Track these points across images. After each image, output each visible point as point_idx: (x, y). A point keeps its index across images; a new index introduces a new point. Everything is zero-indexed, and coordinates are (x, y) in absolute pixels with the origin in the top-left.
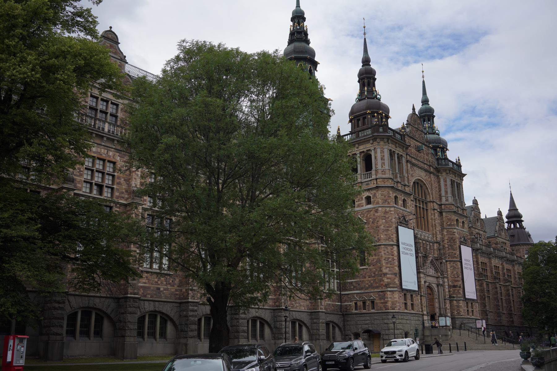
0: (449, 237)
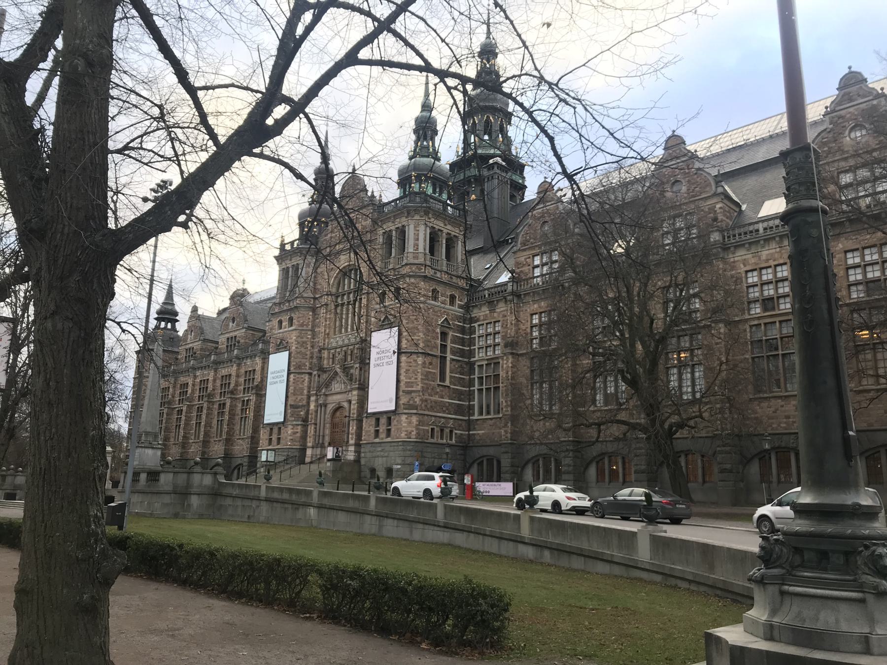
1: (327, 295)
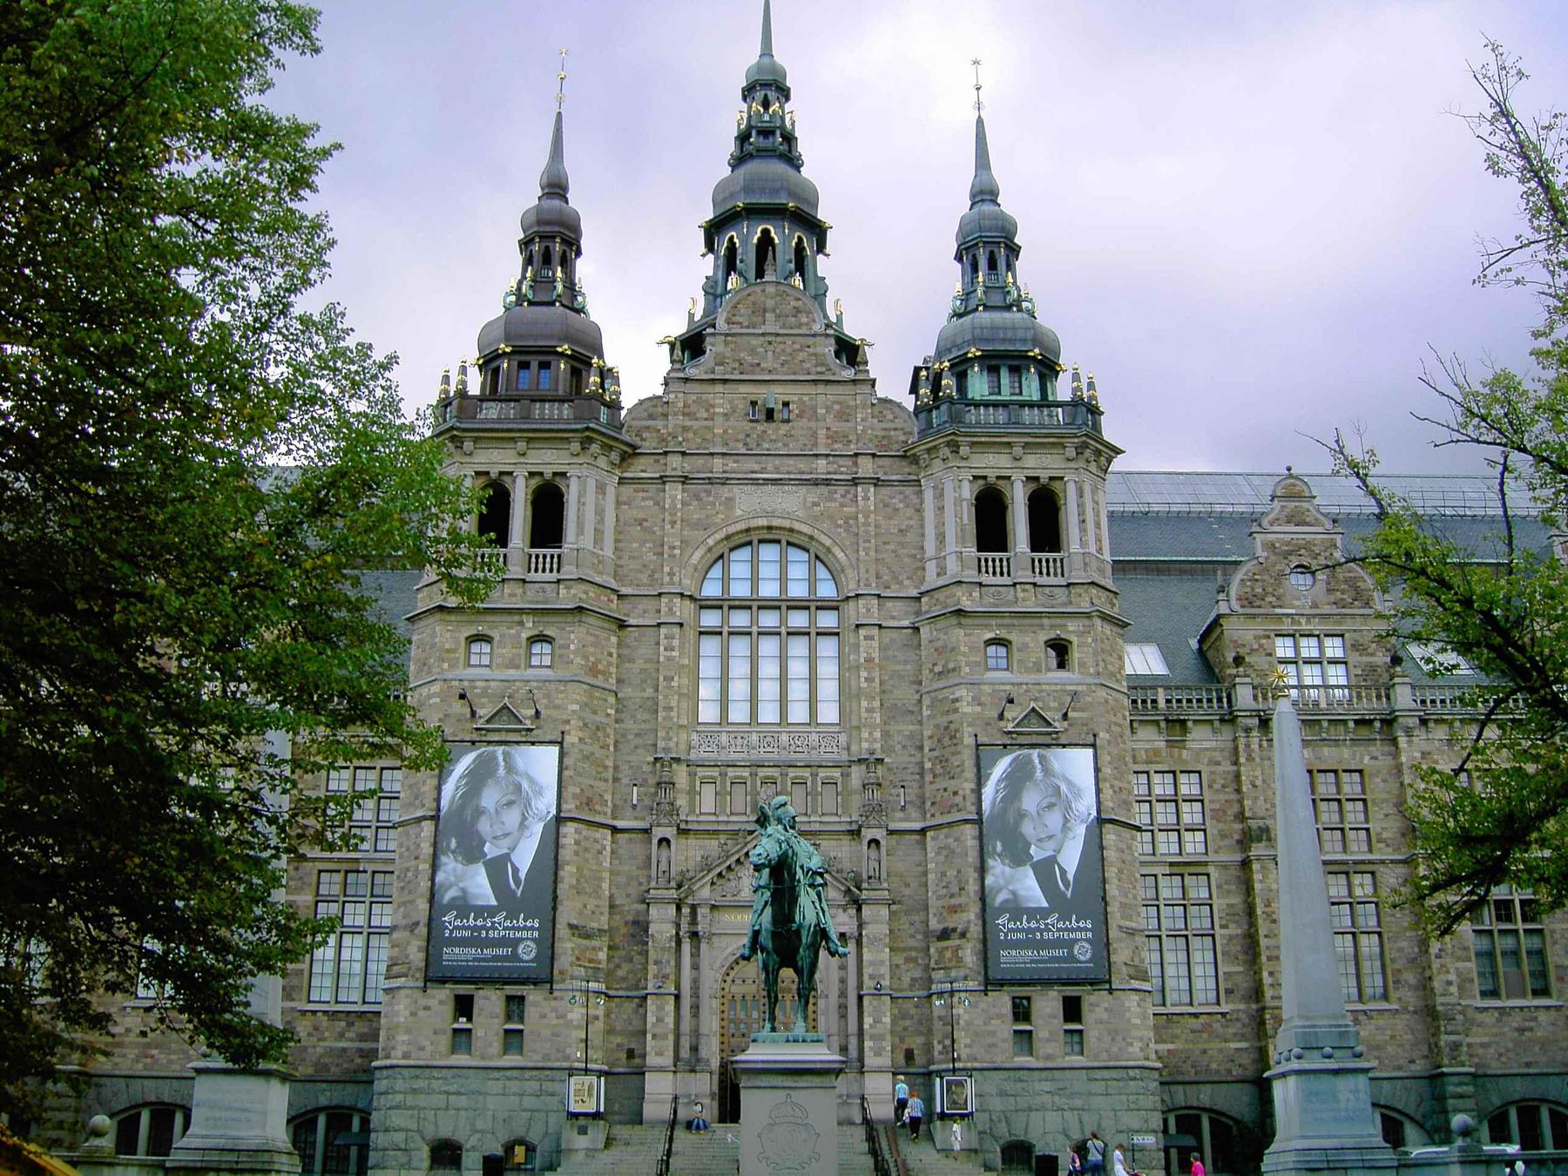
0: (937, 726)
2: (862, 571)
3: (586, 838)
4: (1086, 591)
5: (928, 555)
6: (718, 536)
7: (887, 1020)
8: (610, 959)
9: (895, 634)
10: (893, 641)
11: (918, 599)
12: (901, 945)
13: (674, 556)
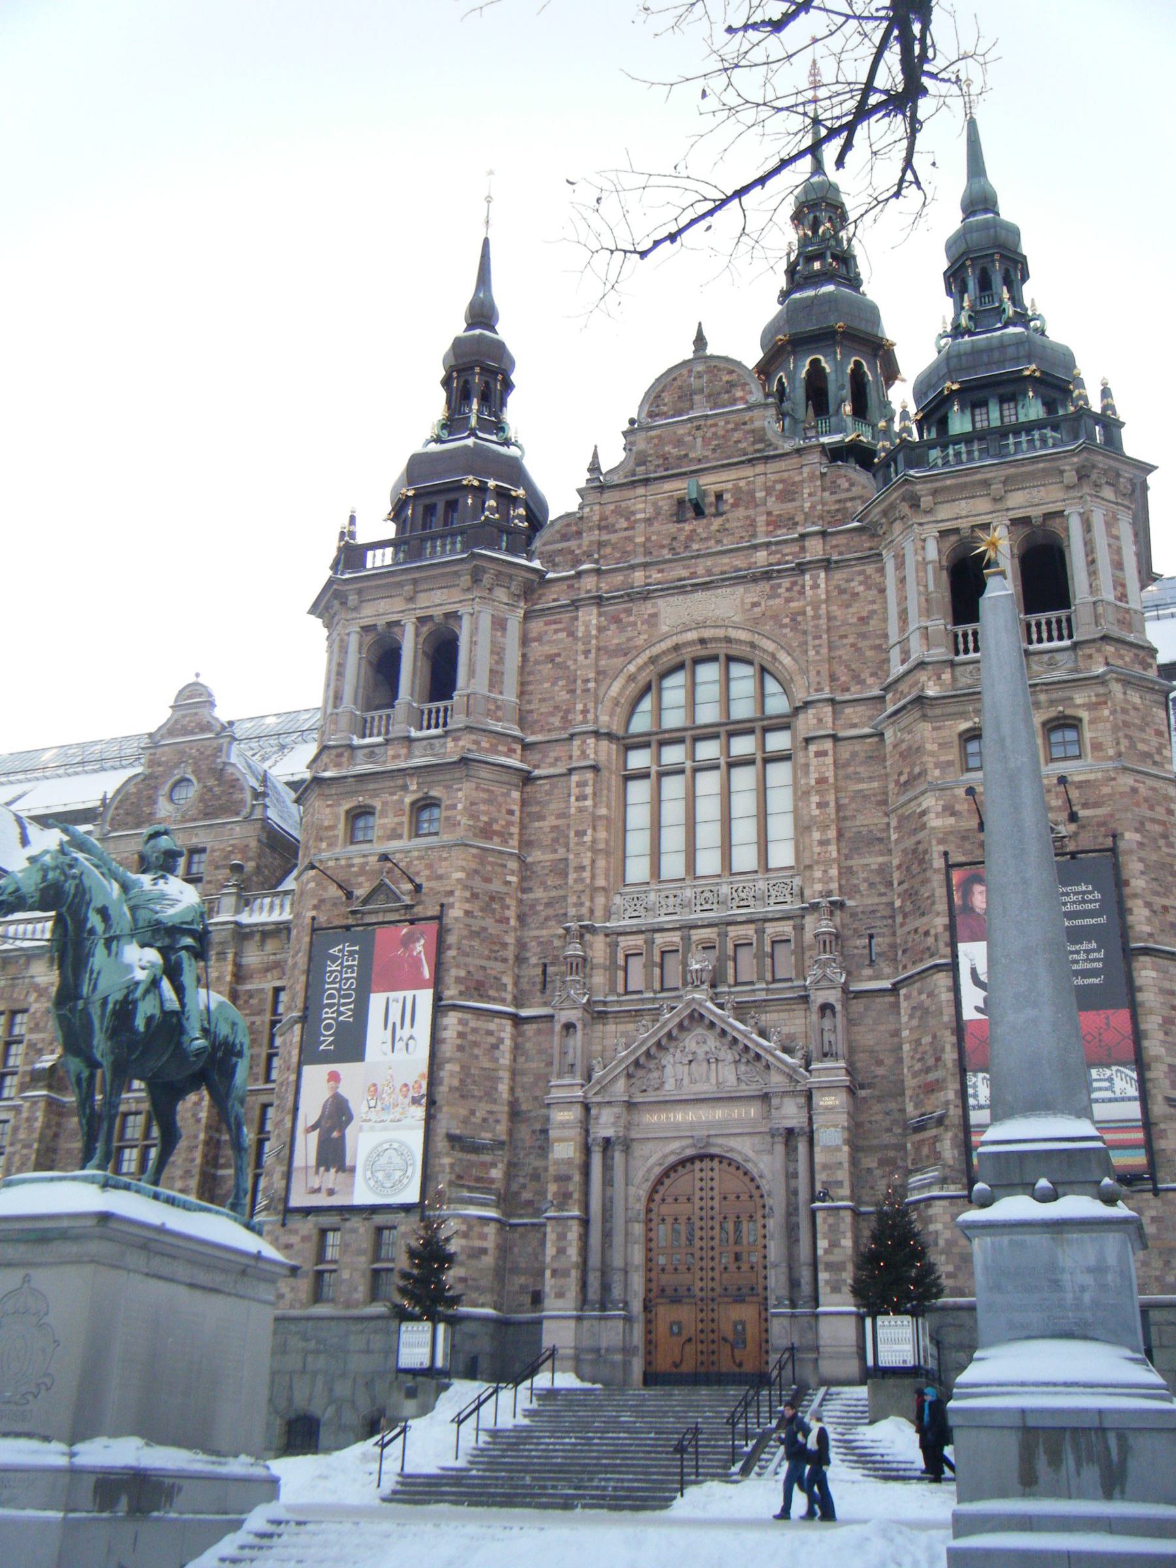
0: (904, 851)
1: (596, 734)
2: (813, 673)
3: (475, 1030)
4: (1099, 650)
5: (892, 641)
6: (640, 661)
7: (847, 1242)
8: (509, 1176)
9: (858, 748)
10: (854, 755)
11: (882, 699)
12: (875, 1142)
13: (588, 690)
